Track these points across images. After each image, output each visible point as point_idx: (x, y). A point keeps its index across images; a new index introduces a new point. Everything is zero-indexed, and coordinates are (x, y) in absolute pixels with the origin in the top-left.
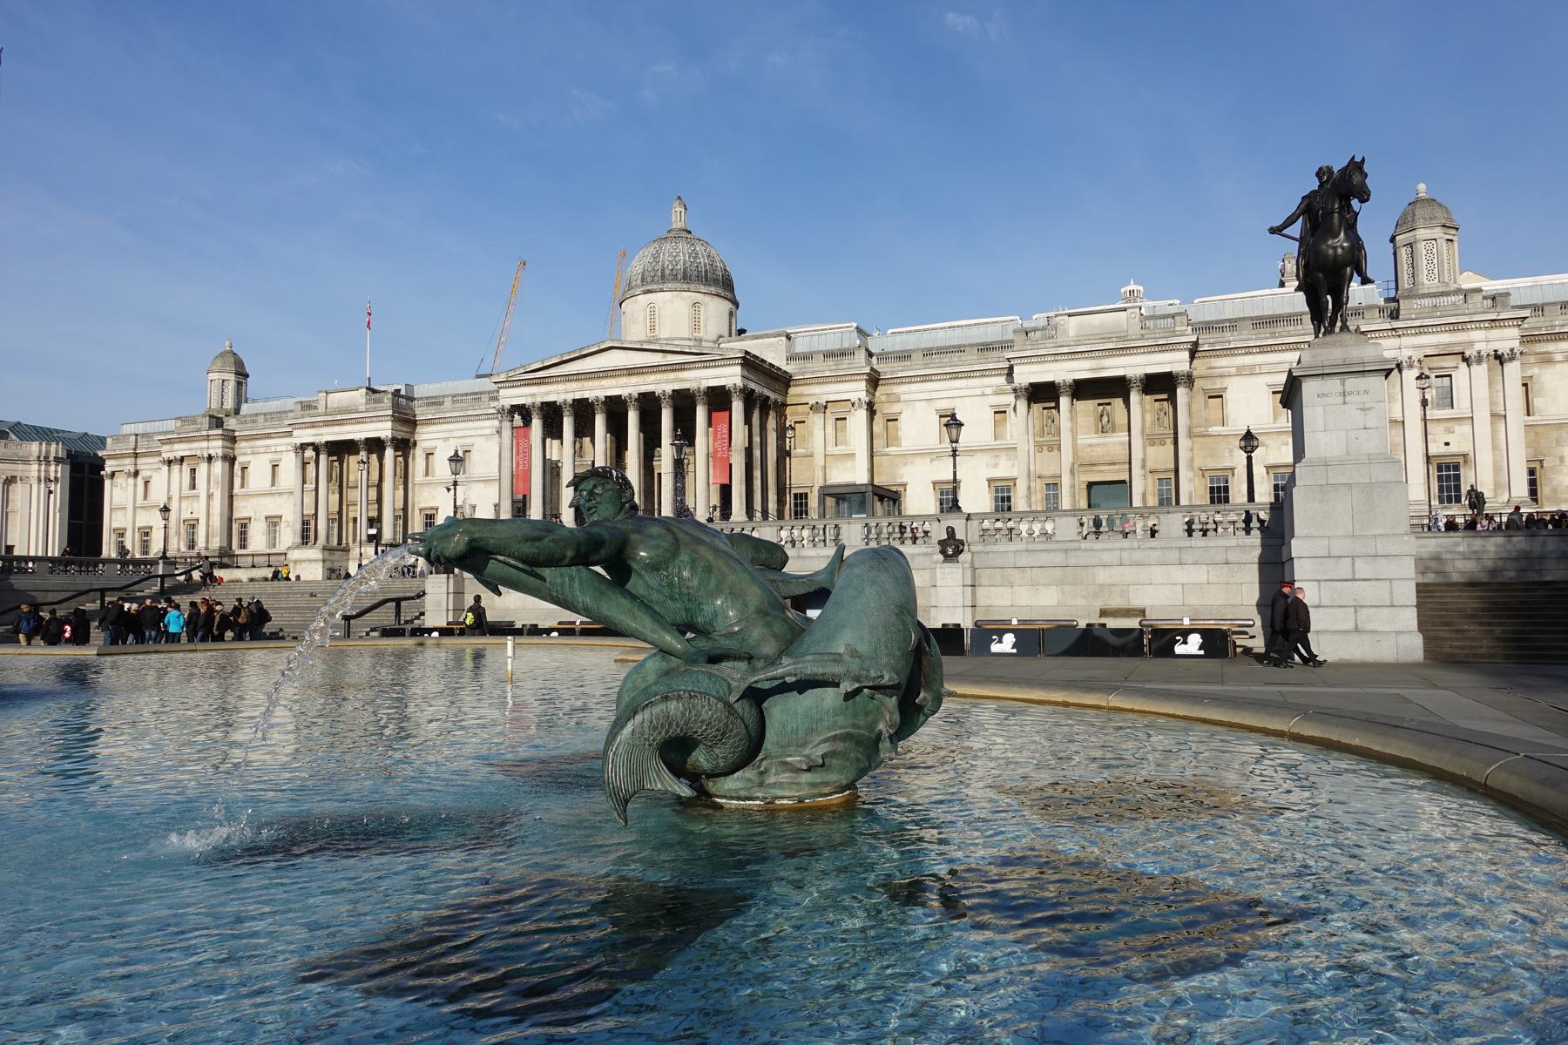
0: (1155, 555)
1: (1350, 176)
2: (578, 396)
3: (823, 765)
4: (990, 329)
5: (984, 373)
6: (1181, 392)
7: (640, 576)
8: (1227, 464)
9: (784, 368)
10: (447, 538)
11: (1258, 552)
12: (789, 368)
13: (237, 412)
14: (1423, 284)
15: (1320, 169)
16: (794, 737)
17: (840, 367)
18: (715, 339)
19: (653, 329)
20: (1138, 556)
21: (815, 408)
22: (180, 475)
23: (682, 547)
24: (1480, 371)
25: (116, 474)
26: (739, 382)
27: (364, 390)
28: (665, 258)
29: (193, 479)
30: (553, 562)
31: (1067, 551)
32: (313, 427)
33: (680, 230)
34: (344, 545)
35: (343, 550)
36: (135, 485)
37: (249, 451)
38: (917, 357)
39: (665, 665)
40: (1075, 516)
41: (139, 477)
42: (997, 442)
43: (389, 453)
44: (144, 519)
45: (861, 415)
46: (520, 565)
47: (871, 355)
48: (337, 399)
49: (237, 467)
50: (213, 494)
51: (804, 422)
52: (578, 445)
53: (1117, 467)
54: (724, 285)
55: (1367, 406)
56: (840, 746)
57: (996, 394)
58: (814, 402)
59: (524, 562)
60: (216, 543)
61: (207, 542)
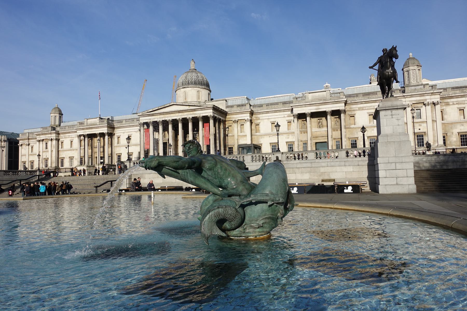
0: (338, 163)
1: (392, 51)
2: (163, 119)
3: (262, 226)
4: (286, 97)
5: (284, 111)
6: (342, 115)
7: (206, 172)
8: (356, 136)
9: (225, 110)
10: (152, 161)
11: (367, 162)
12: (227, 110)
13: (60, 125)
14: (412, 83)
15: (384, 49)
16: (254, 218)
17: (242, 109)
18: (204, 101)
19: (186, 99)
20: (333, 164)
21: (235, 122)
22: (43, 145)
23: (218, 163)
24: (429, 108)
26: (212, 114)
27: (99, 118)
28: (189, 78)
29: (47, 146)
30: (182, 168)
32: (83, 130)
33: (193, 69)
34: (93, 165)
35: (93, 167)
36: (29, 148)
37: (63, 137)
39: (215, 198)
40: (314, 152)
41: (30, 146)
42: (289, 131)
43: (106, 137)
44: (31, 158)
45: (249, 123)
46: (173, 169)
47: (251, 106)
48: (90, 121)
50: (53, 150)
51: (231, 126)
52: (164, 134)
53: (324, 138)
54: (207, 86)
55: (399, 118)
56: (267, 221)
57: (288, 117)
58: (234, 120)
59: (174, 168)
60: (54, 165)
61: (51, 165)
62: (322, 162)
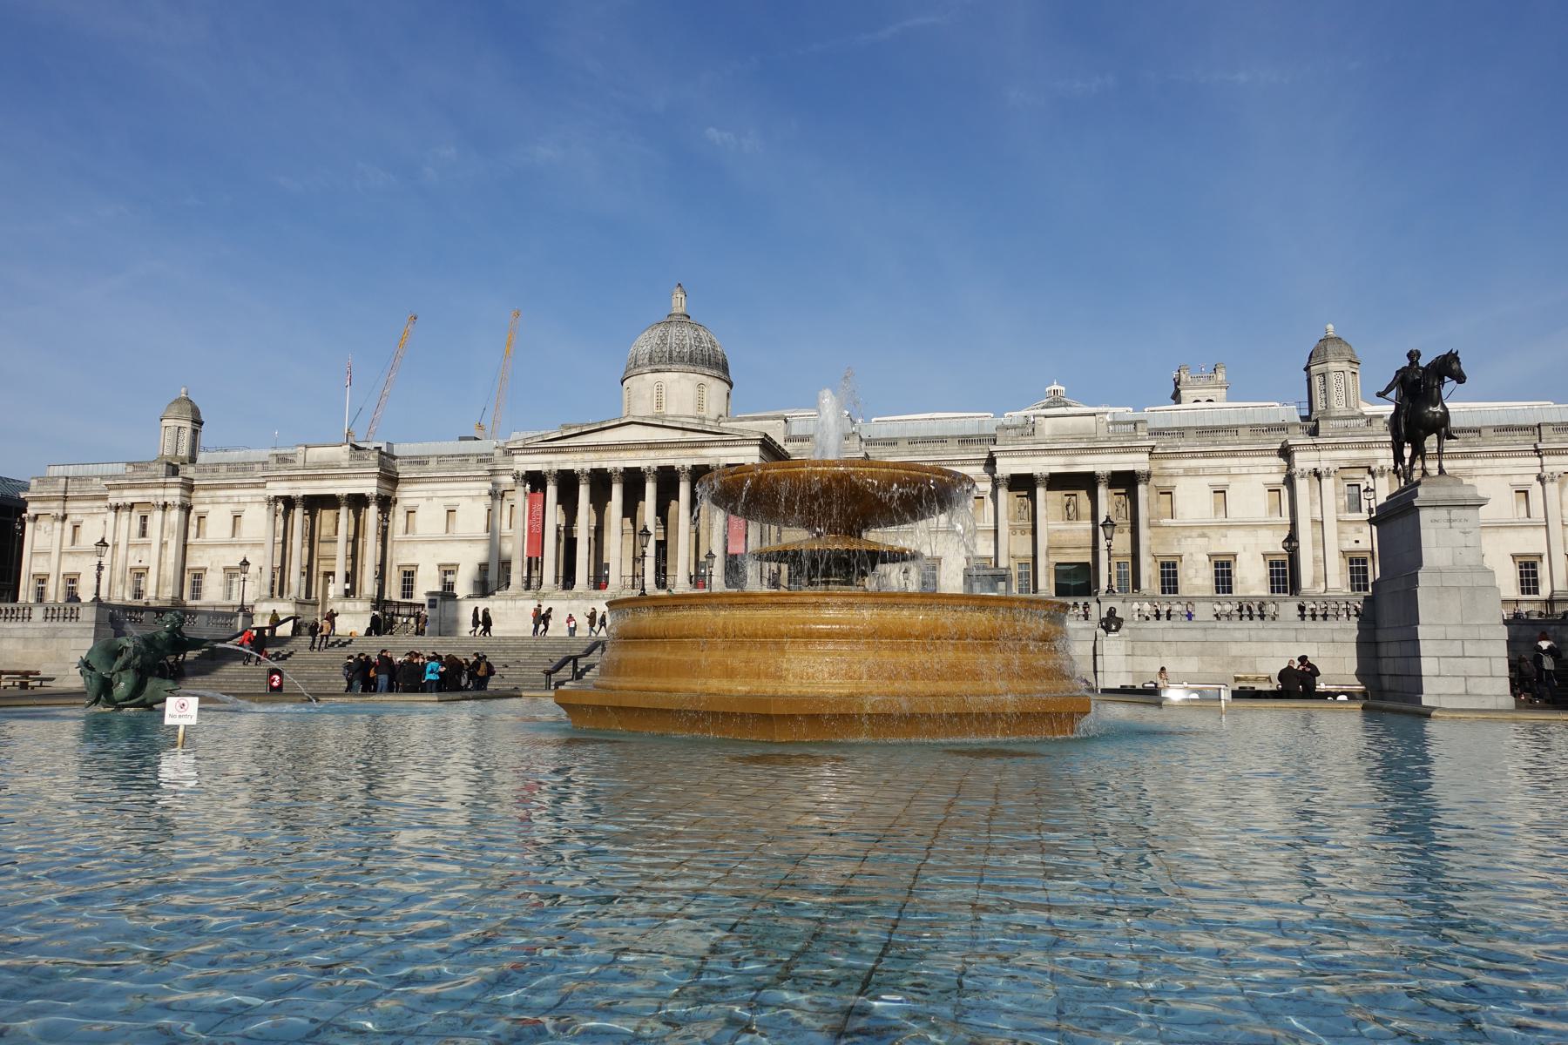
0: (1277, 634)
1: (1450, 363)
2: (595, 466)
6: (1141, 488)
8: (1176, 552)
11: (1357, 633)
15: (1411, 351)
19: (659, 405)
20: (1264, 634)
22: (128, 524)
25: (40, 517)
26: (757, 460)
31: (1205, 629)
34: (313, 599)
35: (312, 604)
36: (63, 530)
37: (207, 500)
38: (903, 444)
41: (68, 522)
44: (69, 566)
47: (861, 440)
48: (316, 454)
49: (193, 516)
50: (166, 543)
53: (1082, 550)
54: (718, 366)
60: (168, 593)
62: (1235, 629)
